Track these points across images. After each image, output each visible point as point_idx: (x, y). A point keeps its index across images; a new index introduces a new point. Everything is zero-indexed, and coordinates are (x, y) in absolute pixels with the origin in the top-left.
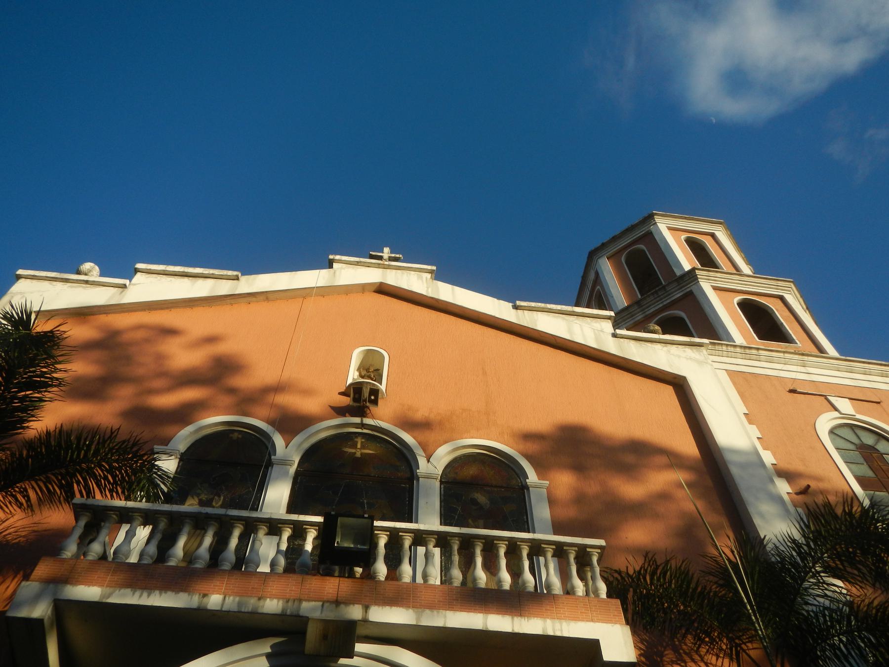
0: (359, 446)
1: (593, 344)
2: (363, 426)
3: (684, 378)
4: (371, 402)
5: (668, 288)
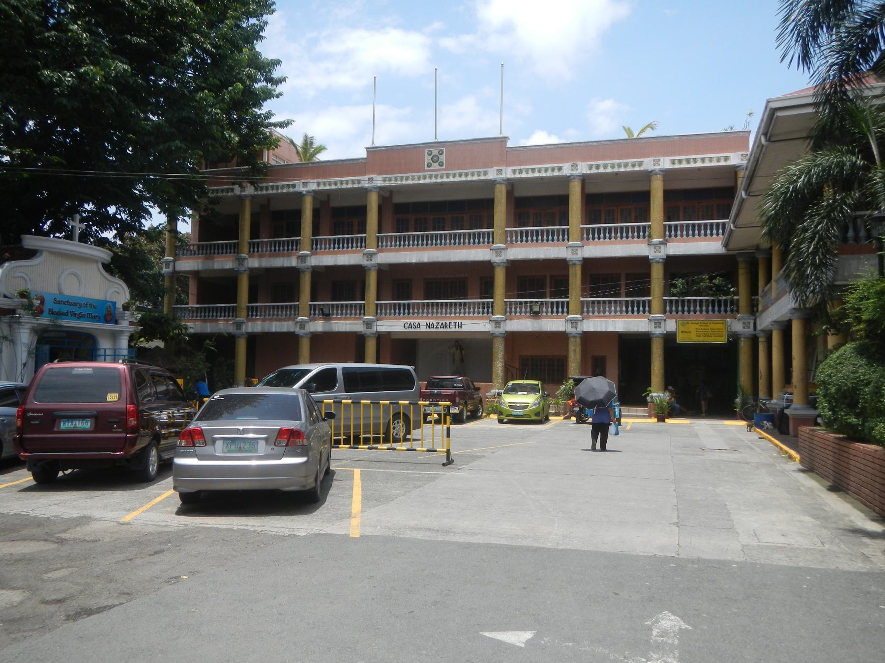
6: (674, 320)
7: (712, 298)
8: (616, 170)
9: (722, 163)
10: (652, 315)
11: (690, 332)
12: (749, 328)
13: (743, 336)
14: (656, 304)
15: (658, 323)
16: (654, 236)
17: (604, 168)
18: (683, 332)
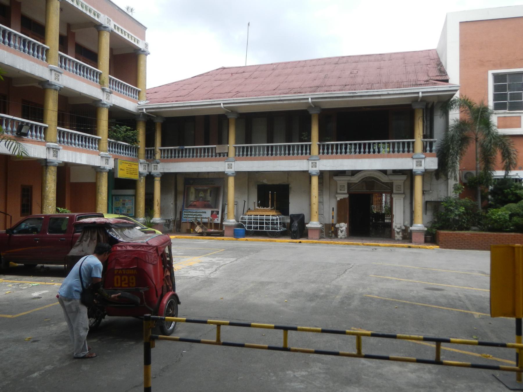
6: (113, 159)
7: (129, 145)
8: (84, 11)
9: (136, 44)
10: (102, 153)
11: (124, 170)
12: (145, 170)
13: (144, 175)
14: (104, 144)
15: (107, 159)
16: (106, 84)
17: (77, 4)
18: (121, 169)
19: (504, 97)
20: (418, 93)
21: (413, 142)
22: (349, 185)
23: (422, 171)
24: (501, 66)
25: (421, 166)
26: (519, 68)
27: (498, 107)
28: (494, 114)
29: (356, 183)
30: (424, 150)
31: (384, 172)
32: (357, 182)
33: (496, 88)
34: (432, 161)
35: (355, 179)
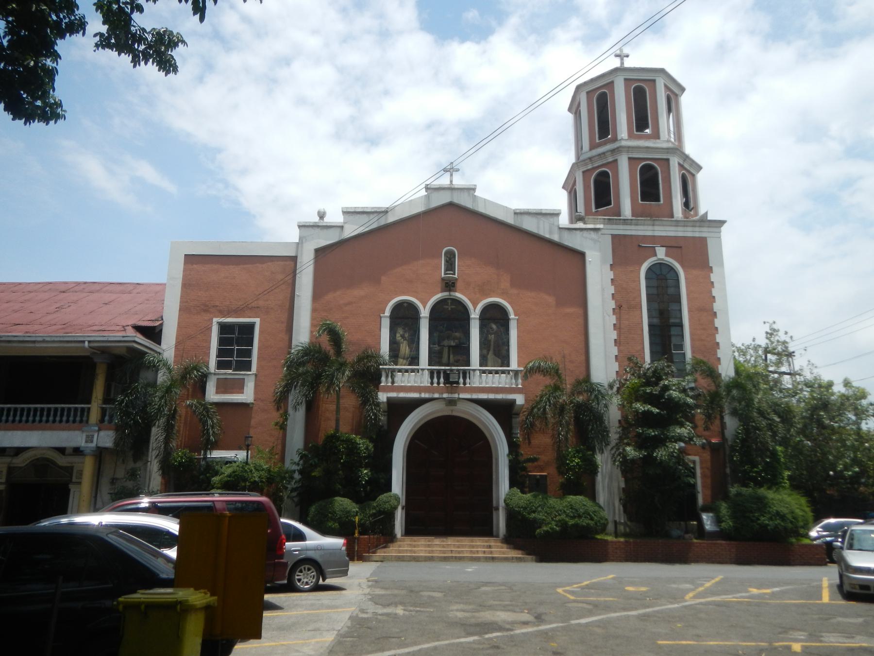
0: (449, 304)
1: (547, 236)
2: (450, 295)
3: (585, 253)
4: (452, 286)
5: (606, 154)
19: (230, 353)
20: (84, 342)
21: (89, 409)
22: (11, 470)
23: (93, 449)
24: (228, 314)
25: (92, 442)
26: (250, 317)
27: (221, 365)
28: (213, 375)
29: (20, 468)
30: (102, 421)
31: (61, 450)
32: (23, 465)
33: (222, 341)
34: (108, 435)
35: (20, 461)
